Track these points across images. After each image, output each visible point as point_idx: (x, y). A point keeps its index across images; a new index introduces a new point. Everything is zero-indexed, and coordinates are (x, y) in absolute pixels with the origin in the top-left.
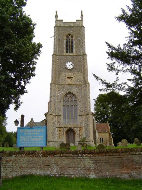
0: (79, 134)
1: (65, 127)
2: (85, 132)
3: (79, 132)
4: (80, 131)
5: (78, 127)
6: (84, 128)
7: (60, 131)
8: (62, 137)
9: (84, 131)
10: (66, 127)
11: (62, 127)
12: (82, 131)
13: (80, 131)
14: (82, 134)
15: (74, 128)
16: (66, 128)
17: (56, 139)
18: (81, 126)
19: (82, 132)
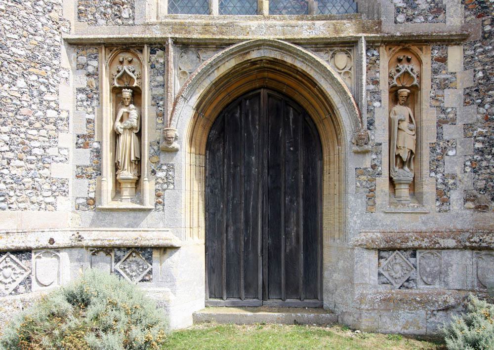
0: (380, 135)
1: (184, 45)
2: (474, 114)
3: (382, 109)
4: (405, 94)
5: (372, 44)
6: (455, 55)
7: (127, 93)
8: (149, 186)
9: (452, 98)
10: (200, 46)
11: (157, 46)
12: (427, 91)
13: (405, 94)
14: (429, 137)
15: (321, 58)
16: (211, 57)
17: (65, 204)
18: (420, 27)
19: (429, 116)
